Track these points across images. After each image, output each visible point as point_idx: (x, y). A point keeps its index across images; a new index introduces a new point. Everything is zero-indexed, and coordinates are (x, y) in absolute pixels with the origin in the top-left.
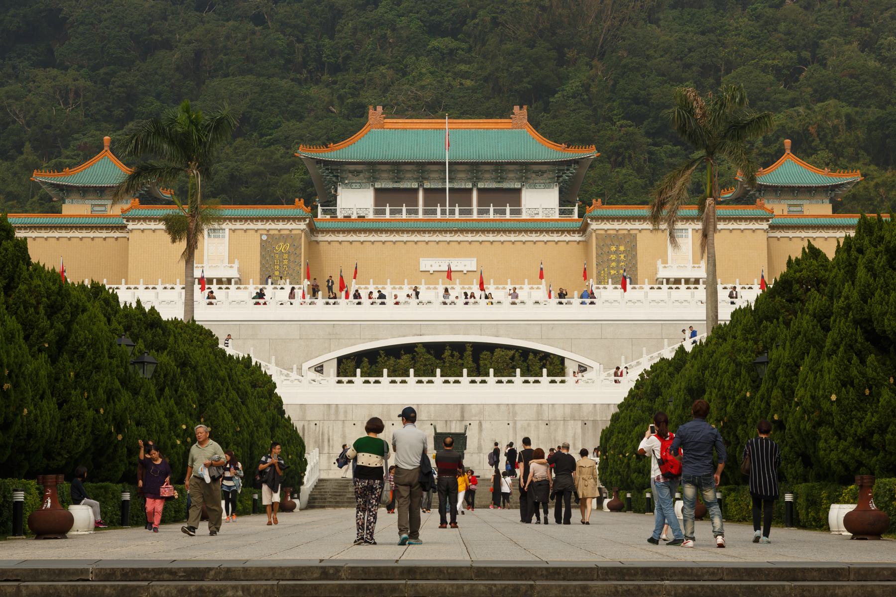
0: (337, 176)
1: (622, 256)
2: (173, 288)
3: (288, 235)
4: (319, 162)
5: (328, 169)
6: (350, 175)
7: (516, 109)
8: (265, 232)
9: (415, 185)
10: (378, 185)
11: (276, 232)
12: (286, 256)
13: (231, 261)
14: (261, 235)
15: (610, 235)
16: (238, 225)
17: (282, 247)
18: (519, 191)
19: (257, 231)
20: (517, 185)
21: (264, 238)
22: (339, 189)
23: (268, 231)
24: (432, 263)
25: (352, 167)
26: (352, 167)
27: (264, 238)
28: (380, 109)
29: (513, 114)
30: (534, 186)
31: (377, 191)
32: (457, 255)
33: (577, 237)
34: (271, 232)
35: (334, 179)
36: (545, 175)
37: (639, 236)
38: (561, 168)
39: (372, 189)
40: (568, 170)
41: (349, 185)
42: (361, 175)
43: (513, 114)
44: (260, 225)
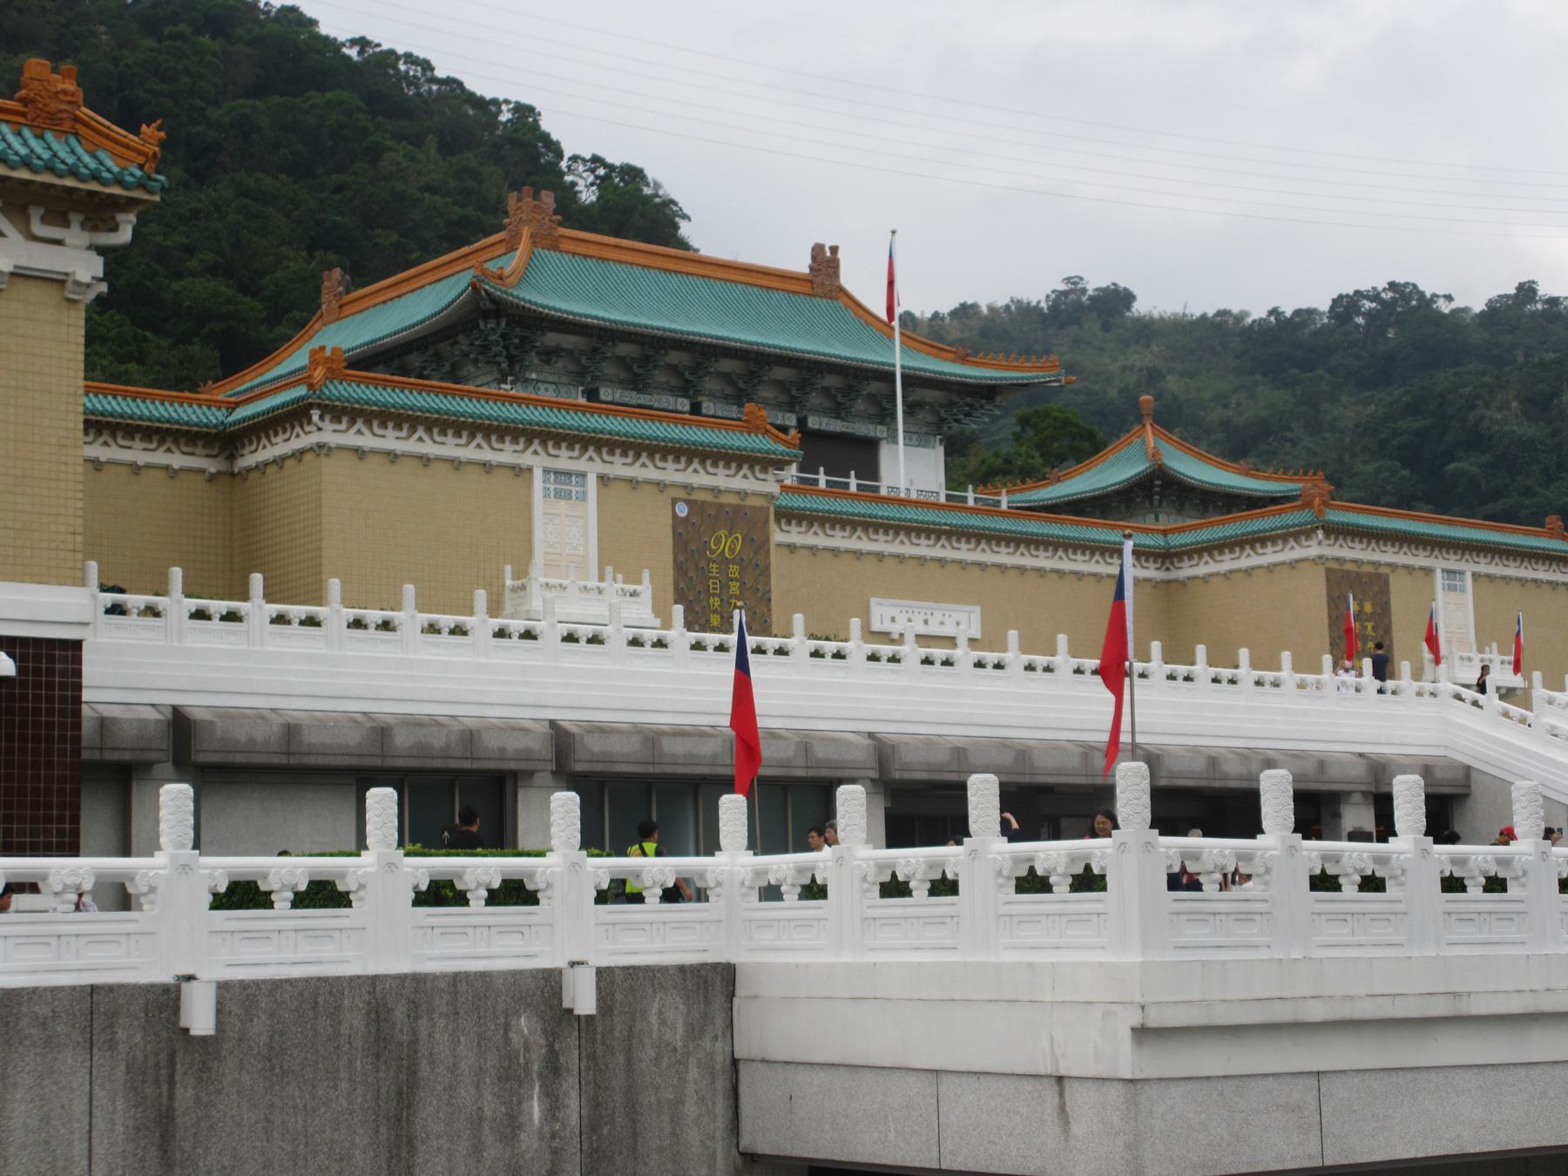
1: (1369, 625)
3: (738, 509)
8: (681, 494)
11: (708, 497)
12: (734, 570)
14: (674, 501)
15: (1347, 572)
16: (619, 467)
17: (726, 543)
19: (661, 486)
21: (682, 510)
23: (688, 488)
24: (895, 612)
27: (682, 510)
32: (940, 596)
34: (700, 496)
37: (1393, 581)
44: (672, 473)
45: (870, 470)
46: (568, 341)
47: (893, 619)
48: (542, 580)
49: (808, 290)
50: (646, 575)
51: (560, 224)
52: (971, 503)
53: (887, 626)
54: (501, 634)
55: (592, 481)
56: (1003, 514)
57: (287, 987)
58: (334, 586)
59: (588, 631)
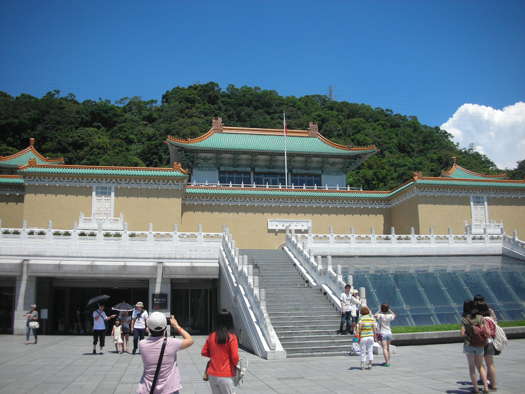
0: (193, 162)
2: (42, 233)
4: (181, 149)
5: (187, 156)
6: (202, 161)
7: (311, 124)
9: (249, 170)
10: (222, 169)
13: (117, 215)
18: (319, 176)
20: (319, 172)
22: (194, 171)
24: (278, 223)
25: (203, 155)
26: (203, 155)
28: (220, 120)
29: (309, 127)
30: (329, 173)
31: (220, 172)
33: (383, 206)
35: (190, 163)
36: (336, 166)
38: (350, 161)
39: (217, 172)
40: (354, 162)
41: (201, 168)
42: (210, 162)
43: (309, 127)
45: (319, 184)
46: (209, 155)
47: (277, 226)
48: (83, 218)
49: (307, 135)
50: (122, 215)
51: (223, 126)
52: (316, 189)
53: (274, 227)
54: (31, 233)
55: (113, 189)
56: (327, 191)
57: (75, 332)
58: (25, 223)
59: (114, 233)
